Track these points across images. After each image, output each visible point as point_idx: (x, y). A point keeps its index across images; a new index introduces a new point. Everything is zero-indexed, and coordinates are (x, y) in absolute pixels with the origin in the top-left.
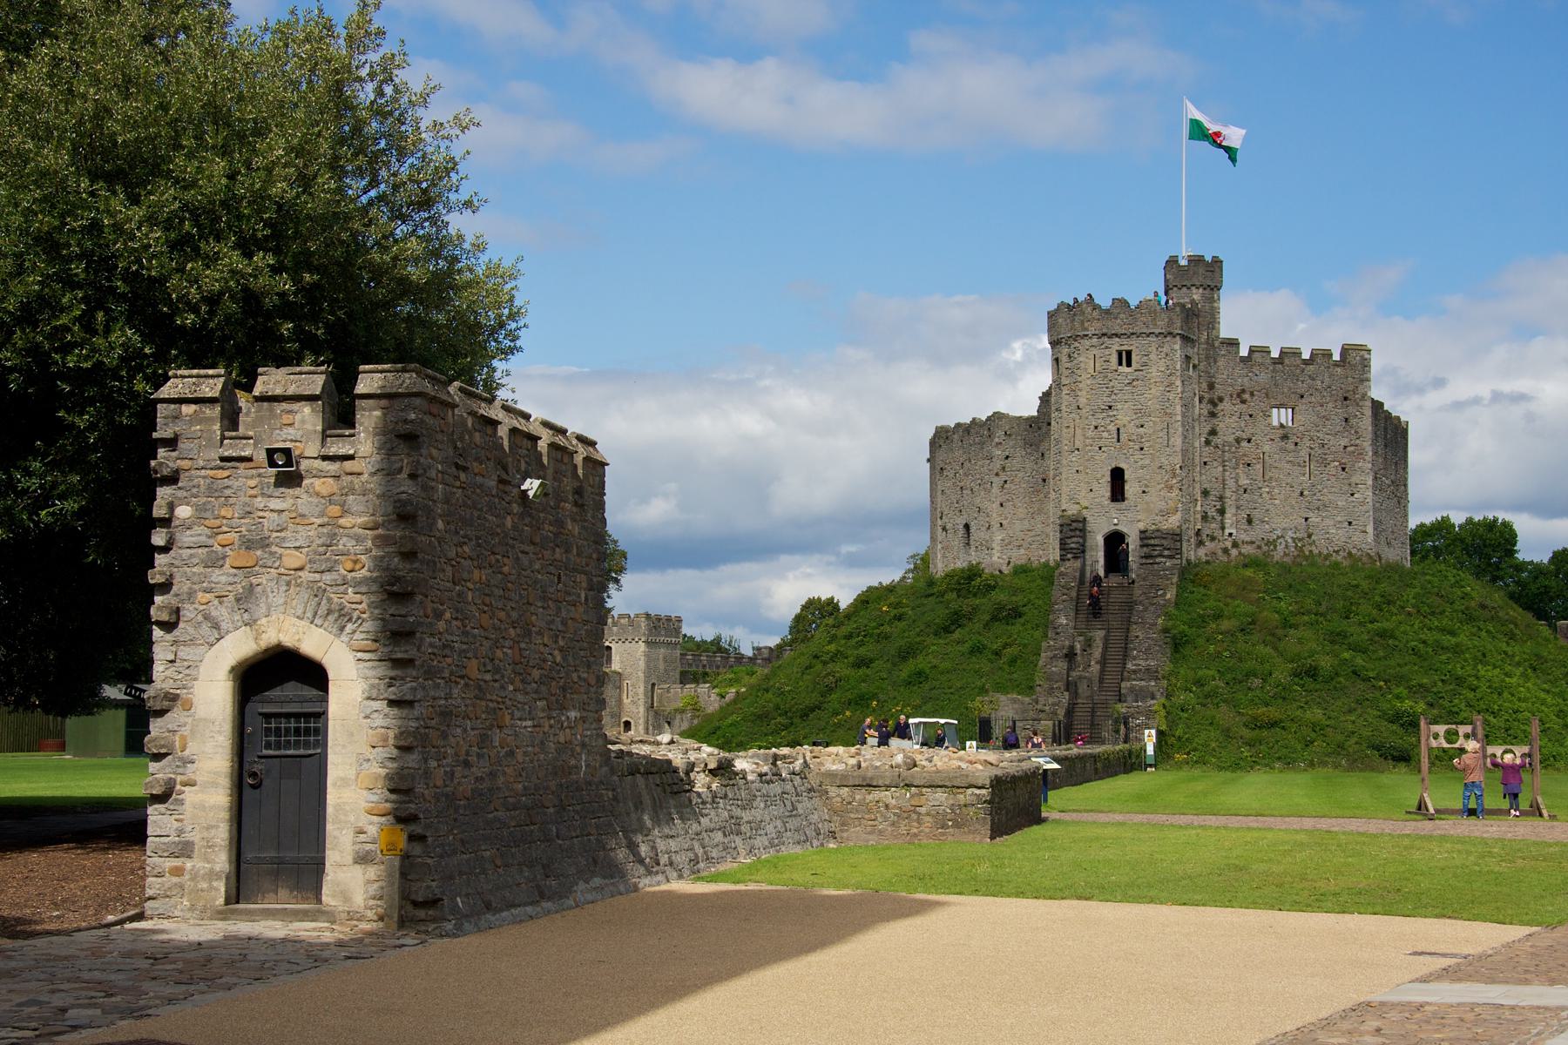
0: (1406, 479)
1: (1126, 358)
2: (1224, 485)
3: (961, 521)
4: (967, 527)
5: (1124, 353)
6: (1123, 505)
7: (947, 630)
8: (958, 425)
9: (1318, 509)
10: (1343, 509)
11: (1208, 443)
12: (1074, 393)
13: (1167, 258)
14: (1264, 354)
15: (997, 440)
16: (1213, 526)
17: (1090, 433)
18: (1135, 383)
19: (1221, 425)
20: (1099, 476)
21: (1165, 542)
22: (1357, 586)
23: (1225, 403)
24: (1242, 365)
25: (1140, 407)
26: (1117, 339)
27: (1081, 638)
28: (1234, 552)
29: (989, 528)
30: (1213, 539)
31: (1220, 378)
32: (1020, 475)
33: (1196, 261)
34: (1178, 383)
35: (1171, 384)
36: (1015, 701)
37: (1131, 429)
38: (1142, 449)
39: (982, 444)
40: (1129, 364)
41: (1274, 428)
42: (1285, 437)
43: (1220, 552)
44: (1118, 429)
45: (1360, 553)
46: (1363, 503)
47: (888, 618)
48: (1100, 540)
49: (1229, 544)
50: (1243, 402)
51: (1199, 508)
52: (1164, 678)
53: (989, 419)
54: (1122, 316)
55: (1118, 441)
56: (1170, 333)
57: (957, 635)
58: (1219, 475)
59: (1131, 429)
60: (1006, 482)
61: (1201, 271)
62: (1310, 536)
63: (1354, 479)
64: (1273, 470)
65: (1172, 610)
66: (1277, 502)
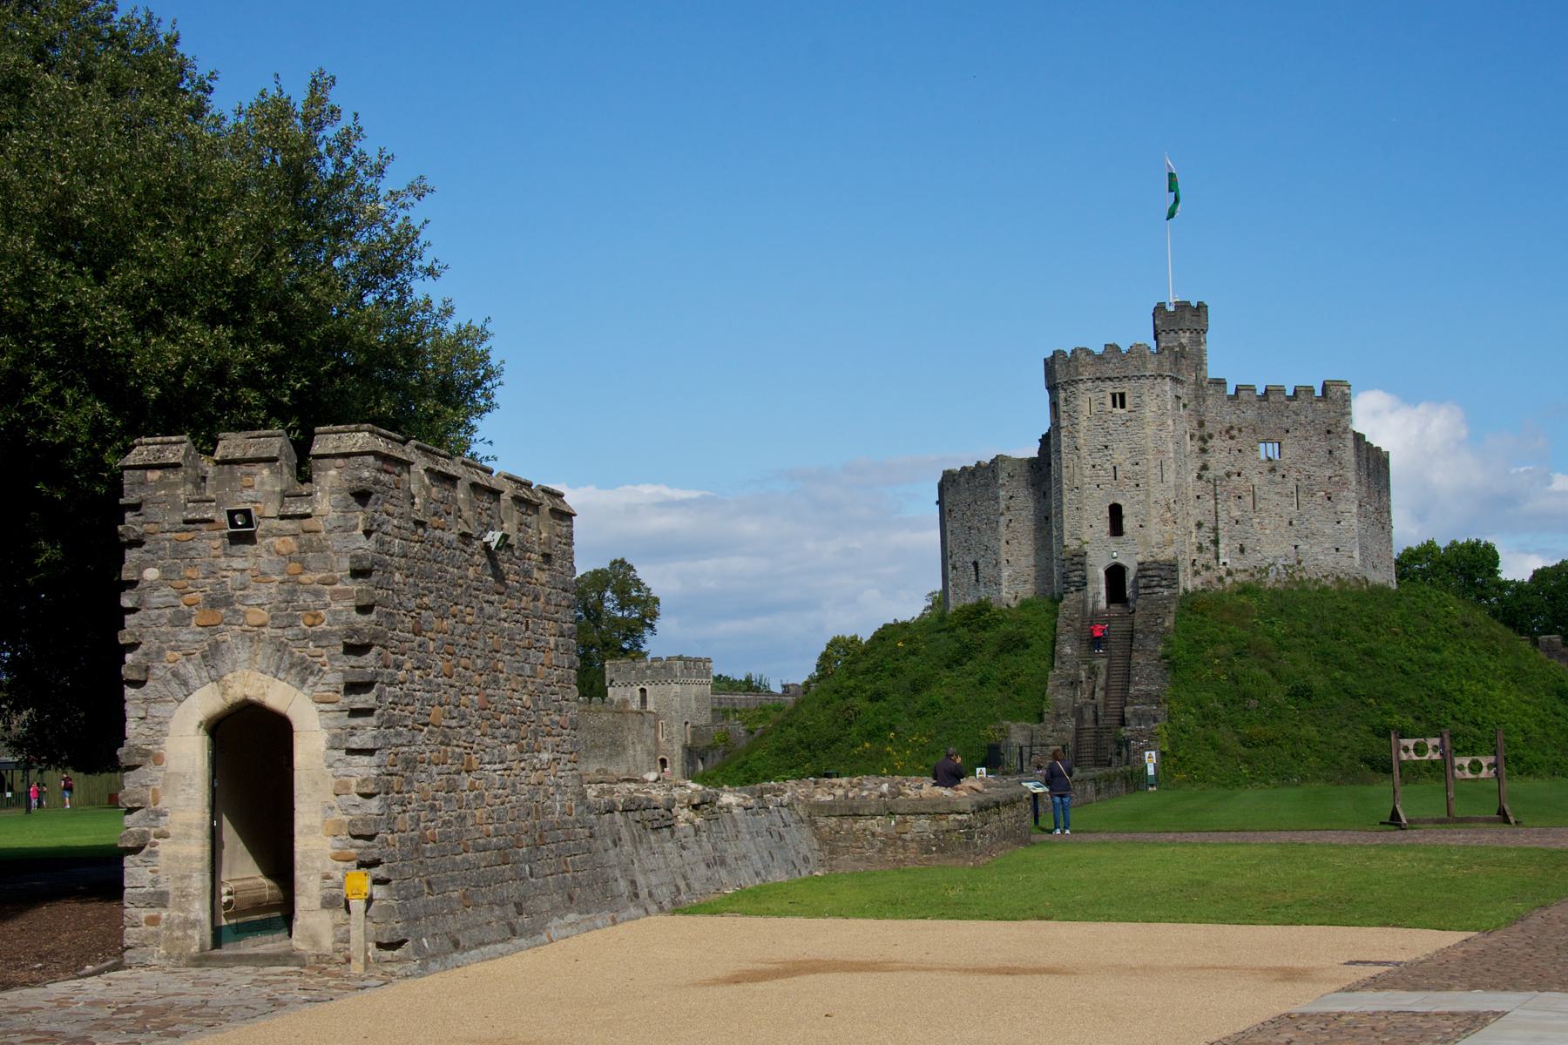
0: (1389, 506)
1: (1120, 400)
2: (1217, 517)
3: (969, 559)
4: (976, 564)
7: (958, 662)
8: (964, 468)
9: (1307, 537)
11: (1200, 477)
13: (1155, 305)
14: (1250, 392)
16: (1208, 556)
18: (1128, 424)
21: (1163, 574)
22: (1346, 609)
23: (1214, 440)
25: (1134, 446)
27: (1087, 667)
28: (1229, 580)
30: (1208, 568)
31: (1209, 416)
32: (1024, 513)
33: (1182, 306)
34: (1170, 422)
35: (1163, 423)
36: (1024, 728)
38: (1138, 485)
39: (987, 485)
40: (1123, 406)
41: (1262, 462)
42: (1273, 470)
43: (1215, 581)
44: (1115, 468)
45: (1347, 577)
46: (1348, 530)
47: (903, 653)
48: (1102, 573)
49: (1223, 574)
50: (1232, 438)
51: (1193, 540)
52: (1165, 701)
53: (992, 461)
54: (1114, 360)
56: (1160, 375)
57: (969, 666)
59: (1127, 466)
60: (1011, 520)
61: (1188, 316)
62: (1299, 562)
63: (1340, 507)
64: (1263, 501)
65: (1172, 637)
66: (1267, 532)
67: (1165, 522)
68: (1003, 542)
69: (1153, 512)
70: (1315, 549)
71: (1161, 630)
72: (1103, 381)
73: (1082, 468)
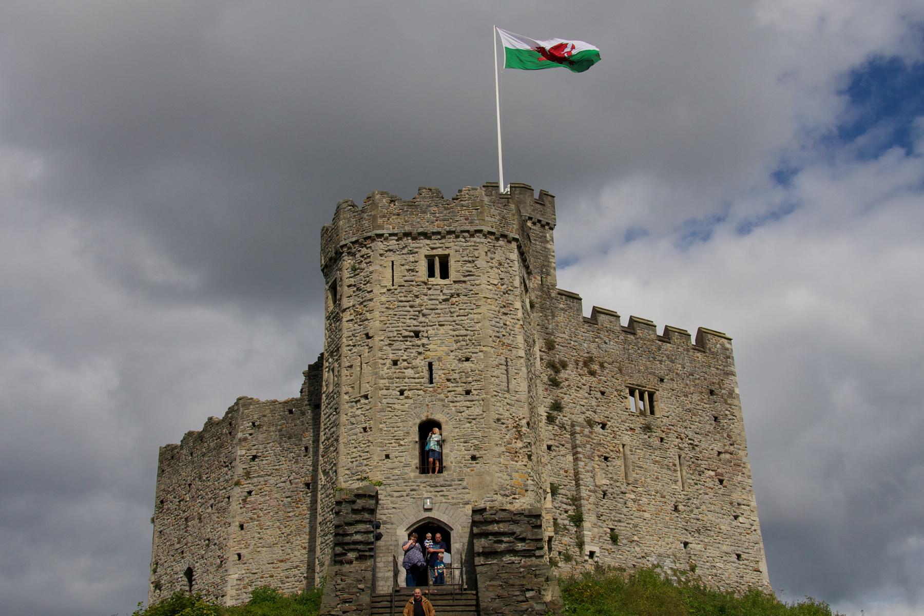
3: (181, 567)
5: (437, 259)
6: (439, 479)
9: (698, 531)
10: (727, 536)
11: (550, 419)
14: (612, 319)
15: (240, 435)
16: (566, 540)
17: (385, 371)
18: (454, 300)
19: (566, 397)
20: (401, 433)
24: (586, 326)
25: (463, 332)
26: (428, 242)
29: (220, 566)
30: (568, 558)
31: (561, 337)
32: (272, 480)
34: (518, 305)
38: (468, 392)
40: (445, 274)
44: (430, 365)
46: (749, 531)
48: (402, 534)
50: (592, 373)
53: (231, 410)
55: (431, 382)
56: (504, 236)
60: (250, 493)
62: (693, 569)
63: (736, 496)
66: (646, 515)
68: (235, 527)
69: (495, 436)
70: (712, 552)
71: (538, 607)
72: (414, 239)
73: (376, 363)
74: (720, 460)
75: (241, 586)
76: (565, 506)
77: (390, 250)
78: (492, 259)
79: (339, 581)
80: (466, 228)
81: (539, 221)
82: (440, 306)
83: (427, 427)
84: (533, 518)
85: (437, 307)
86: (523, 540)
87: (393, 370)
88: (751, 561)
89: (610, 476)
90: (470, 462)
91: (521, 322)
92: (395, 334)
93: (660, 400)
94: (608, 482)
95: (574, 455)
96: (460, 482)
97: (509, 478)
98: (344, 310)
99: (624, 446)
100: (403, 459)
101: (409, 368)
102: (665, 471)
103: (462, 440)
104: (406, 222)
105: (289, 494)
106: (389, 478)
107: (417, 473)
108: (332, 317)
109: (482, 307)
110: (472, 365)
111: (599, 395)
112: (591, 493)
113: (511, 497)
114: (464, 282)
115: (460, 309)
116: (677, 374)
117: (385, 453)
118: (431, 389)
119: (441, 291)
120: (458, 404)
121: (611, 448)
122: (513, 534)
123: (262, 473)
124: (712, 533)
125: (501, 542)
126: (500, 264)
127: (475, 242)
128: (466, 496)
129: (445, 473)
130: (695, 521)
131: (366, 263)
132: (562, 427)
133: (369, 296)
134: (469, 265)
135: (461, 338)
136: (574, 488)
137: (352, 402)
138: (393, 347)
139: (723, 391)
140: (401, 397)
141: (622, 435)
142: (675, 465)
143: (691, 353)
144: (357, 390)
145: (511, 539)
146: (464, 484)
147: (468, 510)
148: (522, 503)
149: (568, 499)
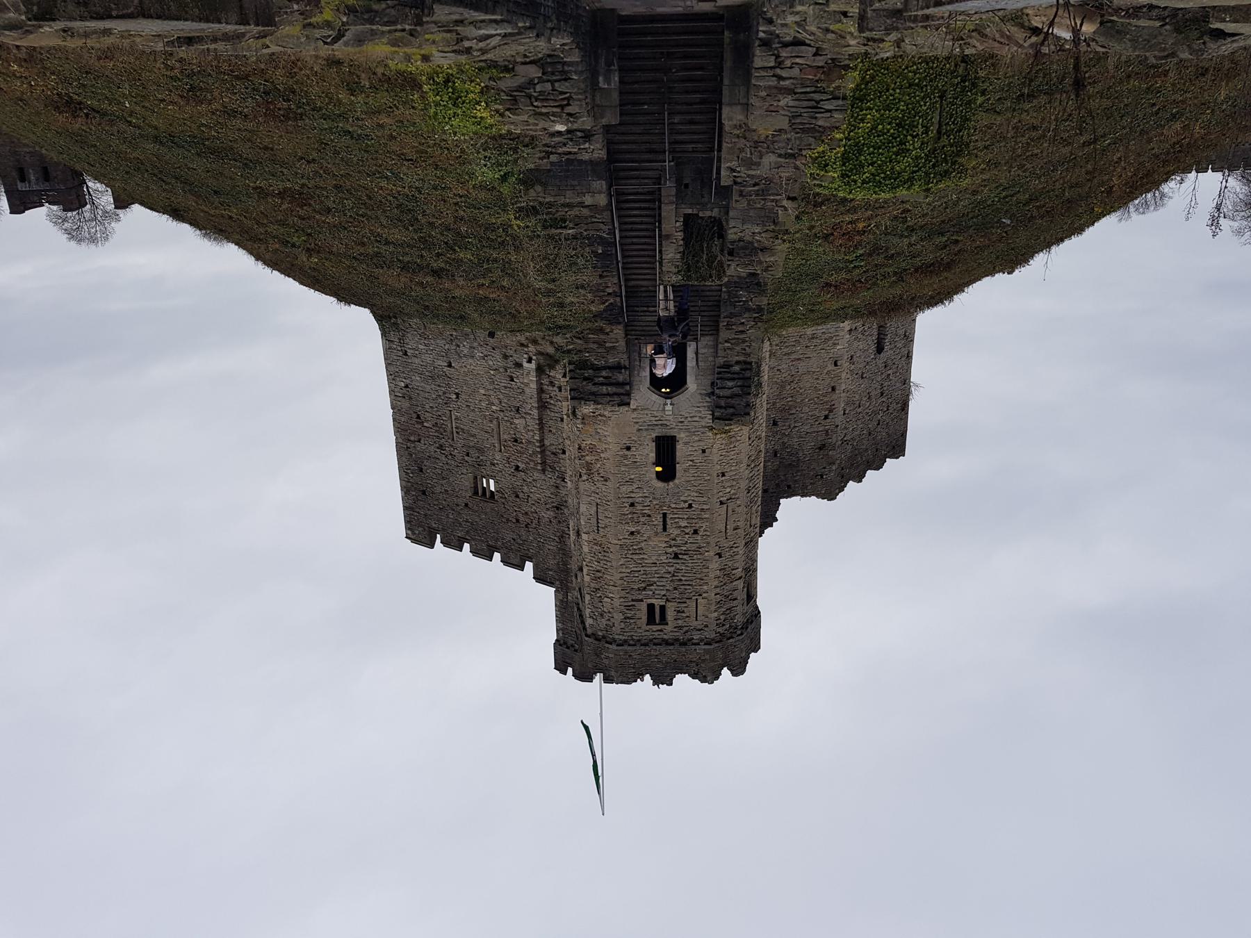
4: (880, 349)
5: (657, 621)
12: (726, 573)
18: (643, 585)
24: (530, 554)
25: (635, 557)
26: (665, 637)
33: (584, 676)
34: (587, 579)
37: (647, 531)
38: (632, 505)
40: (651, 607)
44: (665, 529)
55: (665, 515)
58: (547, 435)
59: (647, 531)
60: (826, 417)
63: (406, 404)
66: (482, 391)
67: (592, 449)
69: (609, 466)
72: (677, 640)
74: (419, 435)
75: (834, 338)
76: (552, 402)
77: (699, 630)
78: (609, 620)
79: (747, 348)
80: (630, 648)
81: (568, 648)
82: (655, 580)
83: (667, 475)
84: (579, 396)
85: (658, 579)
86: (585, 379)
87: (698, 525)
88: (395, 349)
89: (513, 426)
90: (632, 445)
91: (584, 563)
92: (695, 556)
93: (468, 488)
94: (516, 421)
95: (544, 445)
96: (640, 428)
97: (599, 430)
98: (740, 578)
99: (500, 451)
100: (690, 448)
101: (684, 527)
102: (466, 428)
103: (638, 464)
104: (684, 655)
105: (790, 417)
106: (702, 433)
107: (678, 436)
108: (751, 572)
109: (619, 578)
110: (629, 528)
111: (521, 495)
112: (530, 412)
113: (597, 414)
114: (633, 600)
115: (637, 577)
116: (454, 510)
117: (706, 454)
118: (665, 508)
119: (654, 593)
120: (641, 495)
121: (511, 449)
122: (593, 385)
123: (814, 435)
124: (427, 373)
125: (604, 378)
126: (602, 615)
127: (623, 635)
128: (635, 416)
129: (654, 435)
130: (441, 385)
131: (720, 619)
132: (553, 468)
133: (718, 590)
134: (628, 615)
135: (637, 552)
136: (544, 416)
137: (734, 499)
138: (698, 545)
139: (414, 493)
140: (690, 502)
141: (501, 460)
142: (457, 432)
143: (440, 527)
144: (730, 509)
145: (596, 380)
146: (637, 426)
147: (633, 405)
148: (587, 409)
149: (549, 408)
